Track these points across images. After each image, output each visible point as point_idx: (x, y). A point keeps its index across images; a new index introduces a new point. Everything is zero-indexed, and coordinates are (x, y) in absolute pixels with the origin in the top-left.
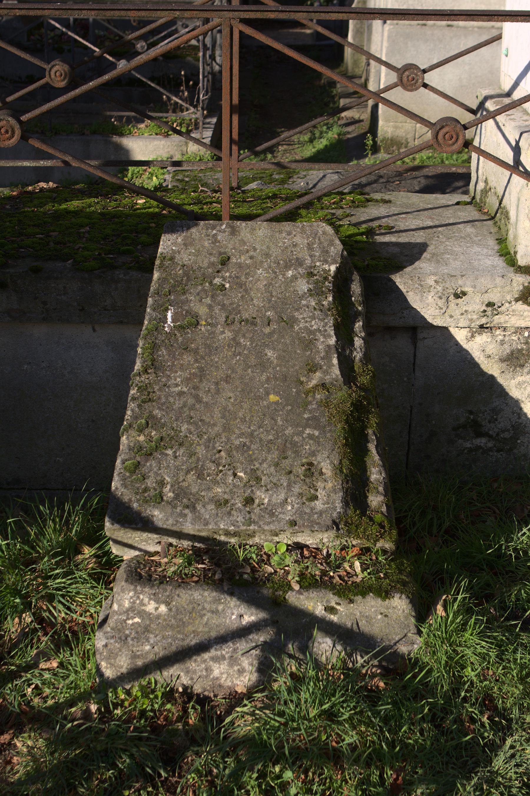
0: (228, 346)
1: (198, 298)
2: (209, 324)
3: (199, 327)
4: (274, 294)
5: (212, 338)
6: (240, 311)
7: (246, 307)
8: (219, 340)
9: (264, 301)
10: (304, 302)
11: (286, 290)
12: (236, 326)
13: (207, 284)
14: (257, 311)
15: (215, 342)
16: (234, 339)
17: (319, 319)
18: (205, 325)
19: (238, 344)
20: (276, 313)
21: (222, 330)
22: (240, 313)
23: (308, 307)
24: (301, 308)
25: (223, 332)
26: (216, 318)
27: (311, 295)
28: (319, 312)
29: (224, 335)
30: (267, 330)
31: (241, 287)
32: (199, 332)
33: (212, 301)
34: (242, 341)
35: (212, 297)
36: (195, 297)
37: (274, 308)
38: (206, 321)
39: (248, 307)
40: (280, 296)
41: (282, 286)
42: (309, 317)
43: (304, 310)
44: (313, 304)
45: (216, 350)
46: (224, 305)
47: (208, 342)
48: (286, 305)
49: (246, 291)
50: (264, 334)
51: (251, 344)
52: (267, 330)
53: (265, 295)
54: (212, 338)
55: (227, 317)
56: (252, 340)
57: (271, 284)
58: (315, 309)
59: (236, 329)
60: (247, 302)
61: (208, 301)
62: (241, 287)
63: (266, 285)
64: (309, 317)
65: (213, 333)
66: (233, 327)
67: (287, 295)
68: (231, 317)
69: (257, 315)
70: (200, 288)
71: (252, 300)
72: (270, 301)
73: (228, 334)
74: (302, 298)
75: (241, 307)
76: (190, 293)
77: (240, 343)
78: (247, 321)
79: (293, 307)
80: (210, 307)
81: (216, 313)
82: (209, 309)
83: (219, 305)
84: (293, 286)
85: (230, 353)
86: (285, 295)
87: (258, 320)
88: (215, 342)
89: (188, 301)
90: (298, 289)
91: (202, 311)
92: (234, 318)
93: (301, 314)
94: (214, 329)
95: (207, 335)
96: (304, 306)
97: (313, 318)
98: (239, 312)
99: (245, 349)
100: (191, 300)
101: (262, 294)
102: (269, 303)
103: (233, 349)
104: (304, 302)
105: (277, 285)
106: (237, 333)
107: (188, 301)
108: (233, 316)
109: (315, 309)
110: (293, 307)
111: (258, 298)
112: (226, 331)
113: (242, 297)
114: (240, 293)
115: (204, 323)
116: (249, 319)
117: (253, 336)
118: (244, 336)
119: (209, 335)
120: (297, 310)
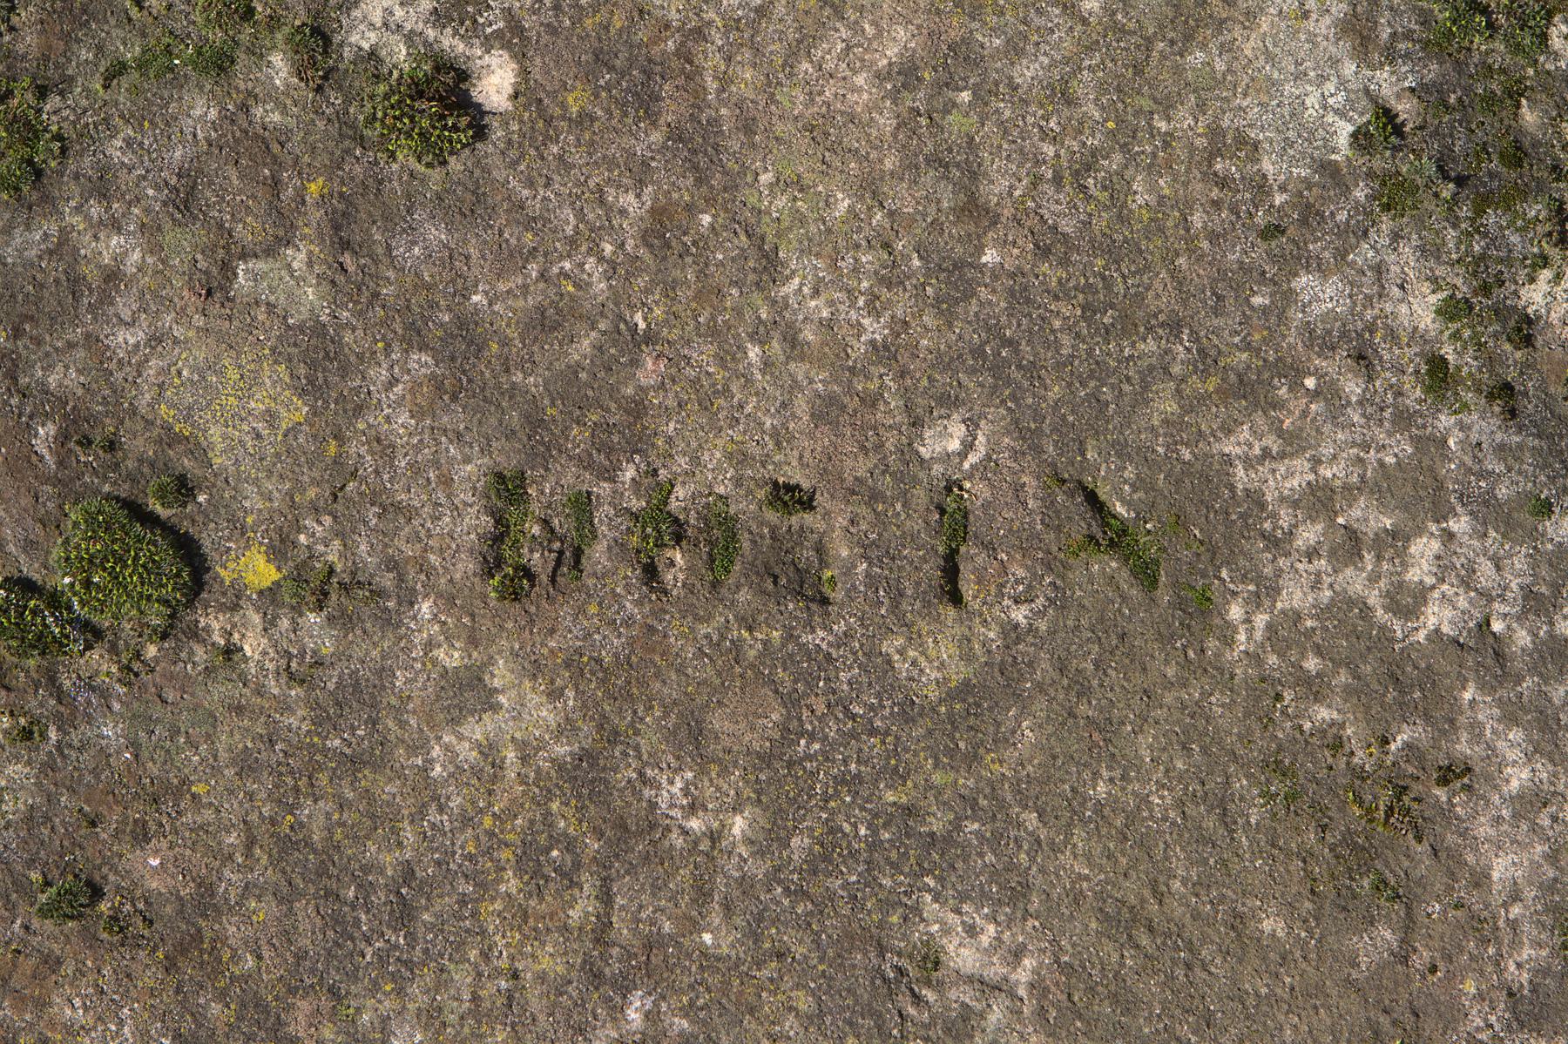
0: (530, 861)
1: (184, 243)
2: (312, 586)
3: (214, 623)
4: (999, 184)
5: (354, 763)
6: (637, 409)
7: (703, 354)
8: (428, 793)
9: (891, 279)
10: (1322, 296)
11: (1125, 137)
12: (603, 611)
13: (279, 68)
14: (826, 411)
15: (380, 819)
16: (585, 776)
17: (1488, 512)
18: (270, 594)
19: (633, 836)
20: (1028, 438)
21: (451, 657)
22: (637, 445)
23: (1363, 359)
24: (1295, 374)
25: (468, 692)
26: (391, 509)
27: (1394, 196)
28: (1485, 425)
29: (476, 730)
30: (935, 657)
31: (646, 105)
32: (219, 692)
33: (335, 282)
34: (671, 790)
35: (341, 235)
36: (150, 231)
37: (999, 366)
38: (279, 551)
39: (729, 357)
40: (1057, 207)
41: (1084, 86)
42: (1381, 485)
43: (1328, 392)
44: (1420, 311)
45: (404, 915)
46: (467, 336)
47: (315, 815)
48: (1127, 327)
49: (697, 146)
50: (908, 712)
51: (772, 839)
52: (935, 657)
53: (904, 198)
54: (354, 763)
55: (507, 489)
56: (777, 780)
57: (963, 54)
58: (1438, 373)
59: (612, 645)
60: (709, 293)
61: (294, 281)
62: (646, 105)
63: (906, 74)
64: (1381, 485)
65: (362, 696)
66: (567, 626)
67: (1141, 196)
68: (549, 489)
69: (827, 468)
70: (200, 110)
71: (770, 267)
72: (956, 278)
73: (527, 715)
74: (1293, 233)
75: (650, 370)
76: (102, 186)
77: (653, 823)
78: (717, 538)
79: (1206, 360)
80: (319, 361)
81: (384, 447)
82: (310, 389)
83: (415, 337)
84: (1206, 89)
85: (548, 960)
86: (1117, 190)
87: (835, 527)
88: (380, 819)
89: (82, 290)
90: (1250, 114)
91: (234, 414)
92: (583, 505)
93: (1294, 443)
94: (369, 650)
95: (297, 721)
96: (1321, 340)
97: (1422, 493)
98: (632, 431)
99: (702, 894)
100: (112, 276)
101: (870, 188)
102: (946, 308)
103: (582, 909)
104: (1322, 296)
105: (1027, 72)
106: (607, 689)
107: (82, 290)
108: (570, 477)
109: (1438, 373)
110: (1206, 360)
111: (830, 244)
112: (501, 674)
113: (661, 228)
114: (640, 174)
115: (260, 570)
116: (743, 507)
117: (788, 734)
118: (692, 738)
119: (323, 721)
120: (1249, 392)
